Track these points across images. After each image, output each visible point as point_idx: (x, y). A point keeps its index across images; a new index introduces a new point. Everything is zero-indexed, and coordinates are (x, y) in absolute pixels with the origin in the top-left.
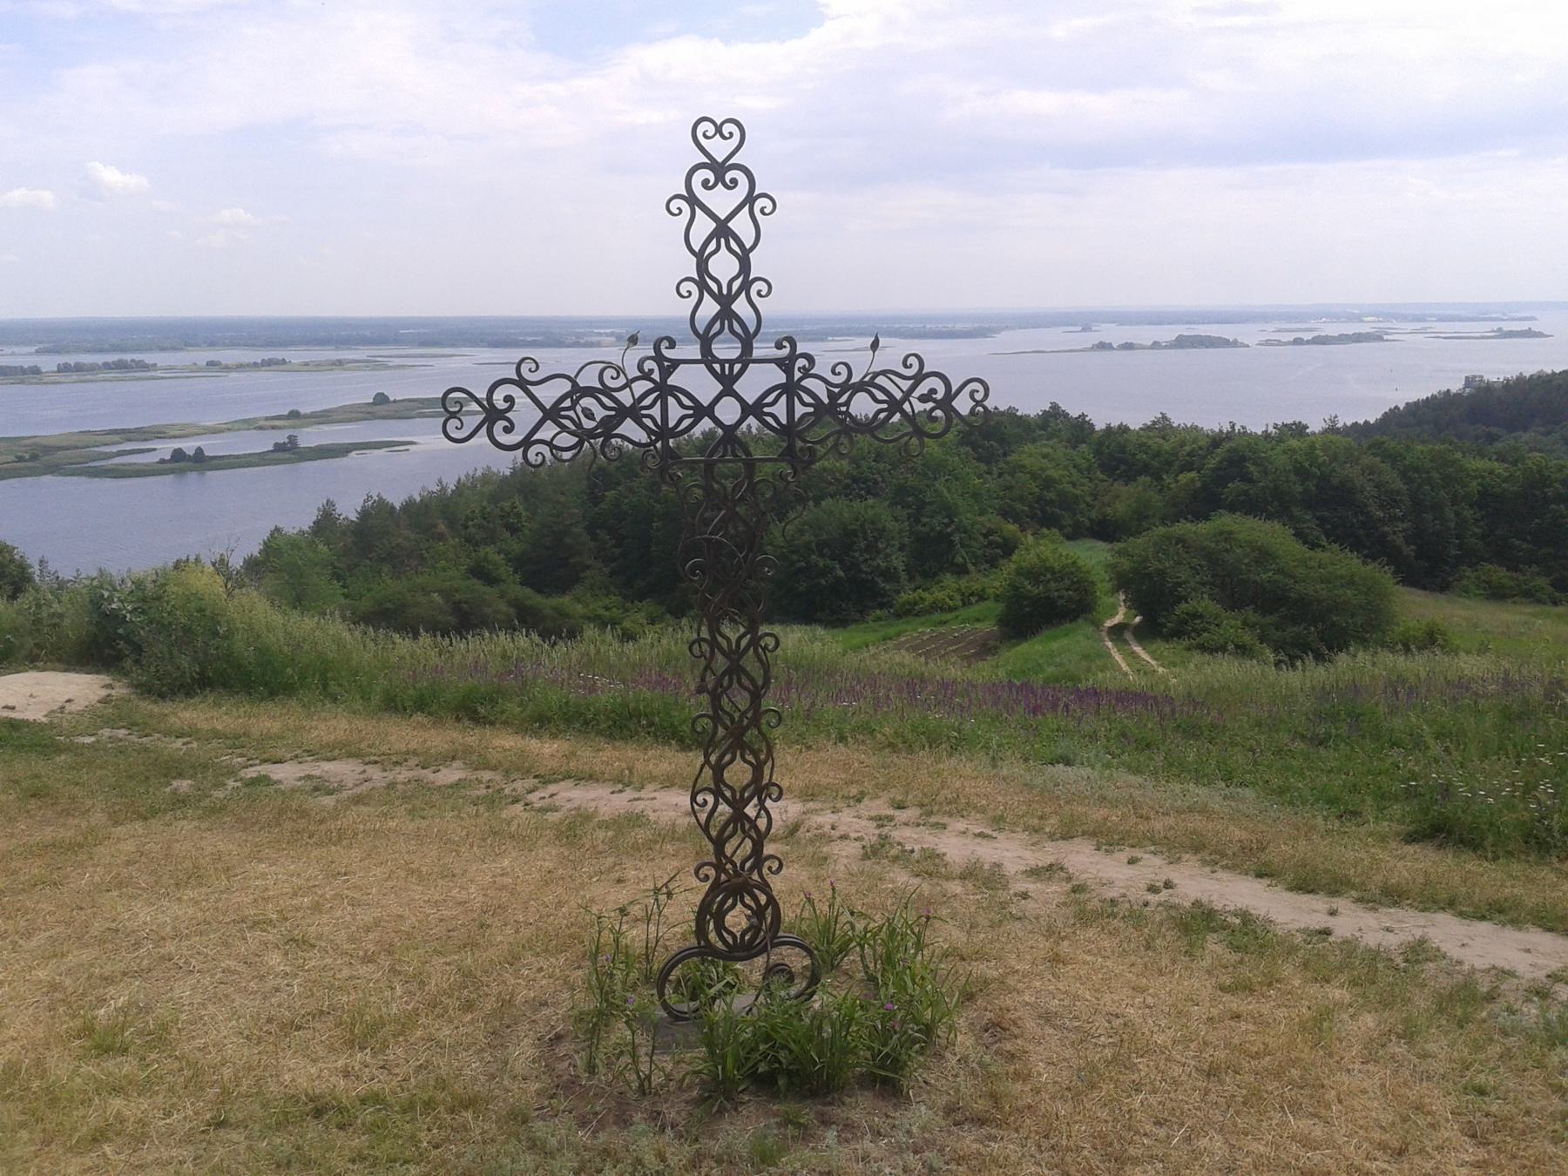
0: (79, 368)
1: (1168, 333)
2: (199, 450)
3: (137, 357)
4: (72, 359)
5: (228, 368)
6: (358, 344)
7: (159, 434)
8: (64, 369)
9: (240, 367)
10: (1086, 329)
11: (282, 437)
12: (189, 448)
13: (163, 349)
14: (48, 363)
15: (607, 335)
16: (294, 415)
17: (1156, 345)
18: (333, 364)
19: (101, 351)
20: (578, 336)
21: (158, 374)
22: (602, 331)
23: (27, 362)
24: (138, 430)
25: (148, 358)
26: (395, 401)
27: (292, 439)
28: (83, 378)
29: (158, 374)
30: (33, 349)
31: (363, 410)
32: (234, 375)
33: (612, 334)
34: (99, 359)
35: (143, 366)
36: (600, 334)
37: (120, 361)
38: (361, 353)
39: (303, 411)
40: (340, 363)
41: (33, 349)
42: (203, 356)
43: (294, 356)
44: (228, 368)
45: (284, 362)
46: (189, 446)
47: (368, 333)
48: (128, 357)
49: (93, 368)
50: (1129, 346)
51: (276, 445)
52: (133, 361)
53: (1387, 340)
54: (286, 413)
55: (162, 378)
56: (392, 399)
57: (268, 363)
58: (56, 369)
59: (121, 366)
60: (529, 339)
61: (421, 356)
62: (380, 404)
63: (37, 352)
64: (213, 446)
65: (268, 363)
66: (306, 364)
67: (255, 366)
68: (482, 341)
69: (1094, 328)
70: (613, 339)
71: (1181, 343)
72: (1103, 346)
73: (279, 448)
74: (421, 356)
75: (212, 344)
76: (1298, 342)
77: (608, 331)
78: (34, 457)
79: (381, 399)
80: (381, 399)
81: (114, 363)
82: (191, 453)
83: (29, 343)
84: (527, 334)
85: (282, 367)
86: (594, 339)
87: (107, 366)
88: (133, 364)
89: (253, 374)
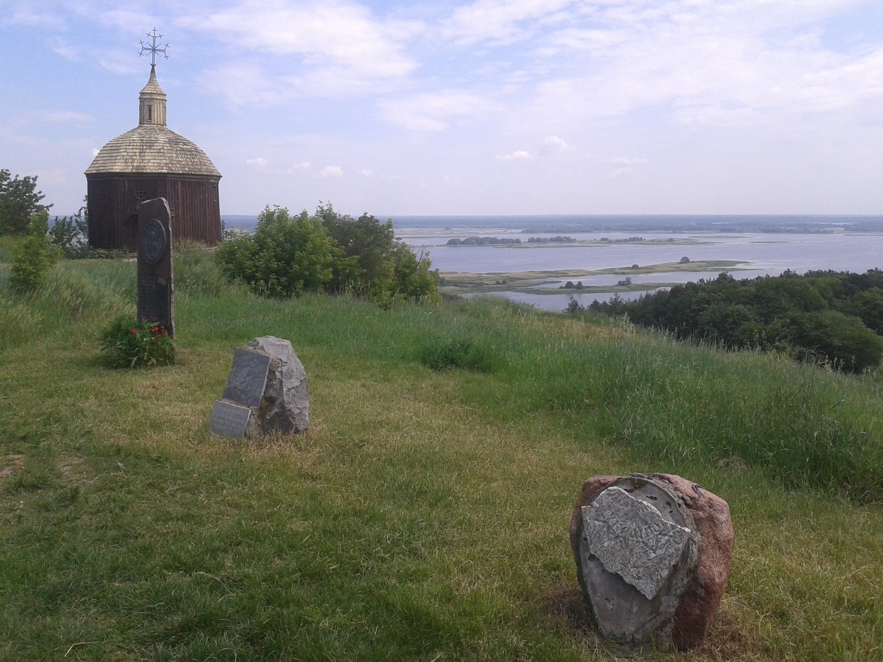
0: (538, 240)
2: (580, 283)
3: (567, 235)
4: (535, 236)
5: (611, 242)
6: (686, 230)
7: (565, 274)
8: (531, 241)
9: (618, 242)
11: (623, 278)
12: (575, 282)
13: (582, 232)
14: (524, 238)
16: (635, 267)
18: (668, 241)
19: (552, 232)
21: (576, 244)
23: (514, 237)
24: (556, 272)
25: (572, 236)
26: (693, 262)
27: (628, 280)
28: (540, 245)
29: (576, 244)
30: (520, 231)
31: (674, 266)
32: (614, 246)
34: (549, 236)
35: (569, 240)
37: (558, 237)
39: (640, 266)
40: (671, 241)
41: (520, 231)
42: (599, 236)
43: (648, 236)
44: (611, 242)
46: (575, 281)
48: (562, 235)
49: (545, 241)
51: (620, 282)
54: (631, 266)
55: (577, 246)
57: (632, 240)
58: (528, 241)
59: (558, 240)
61: (719, 237)
62: (684, 263)
63: (522, 232)
65: (632, 240)
66: (653, 241)
67: (625, 241)
73: (621, 284)
74: (719, 237)
75: (608, 229)
78: (504, 283)
79: (685, 260)
80: (685, 260)
81: (555, 238)
82: (576, 284)
83: (518, 228)
85: (639, 242)
87: (552, 240)
88: (564, 239)
89: (623, 245)
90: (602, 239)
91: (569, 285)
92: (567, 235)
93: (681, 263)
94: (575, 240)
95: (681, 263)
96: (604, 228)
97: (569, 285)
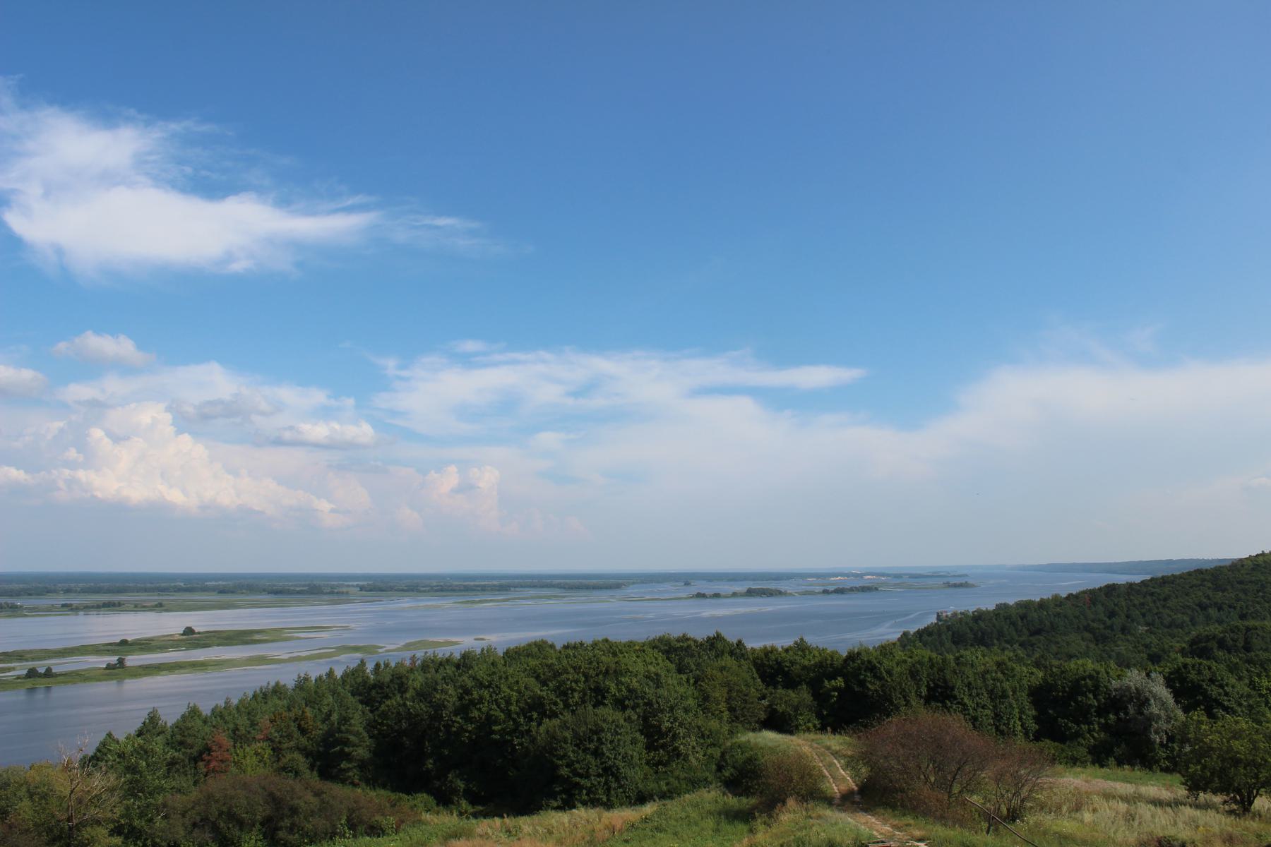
1: (741, 588)
2: (49, 670)
3: (9, 601)
7: (20, 656)
10: (687, 584)
11: (113, 659)
15: (353, 586)
16: (124, 642)
17: (735, 595)
18: (156, 606)
20: (332, 587)
22: (351, 583)
26: (199, 633)
27: (121, 661)
33: (357, 586)
36: (348, 586)
42: (60, 600)
45: (119, 604)
46: (41, 667)
47: (182, 584)
50: (717, 596)
51: (108, 665)
52: (6, 603)
53: (881, 590)
54: (118, 641)
56: (196, 631)
60: (298, 589)
64: (59, 666)
68: (264, 590)
69: (692, 584)
70: (359, 589)
72: (701, 596)
73: (109, 667)
75: (68, 591)
76: (825, 592)
77: (355, 583)
79: (189, 631)
80: (189, 631)
82: (42, 670)
84: (296, 586)
85: (118, 608)
86: (345, 590)
90: (63, 606)
91: (32, 673)
92: (9, 601)
93: (182, 635)
94: (21, 606)
95: (182, 635)
96: (62, 590)
97: (32, 673)
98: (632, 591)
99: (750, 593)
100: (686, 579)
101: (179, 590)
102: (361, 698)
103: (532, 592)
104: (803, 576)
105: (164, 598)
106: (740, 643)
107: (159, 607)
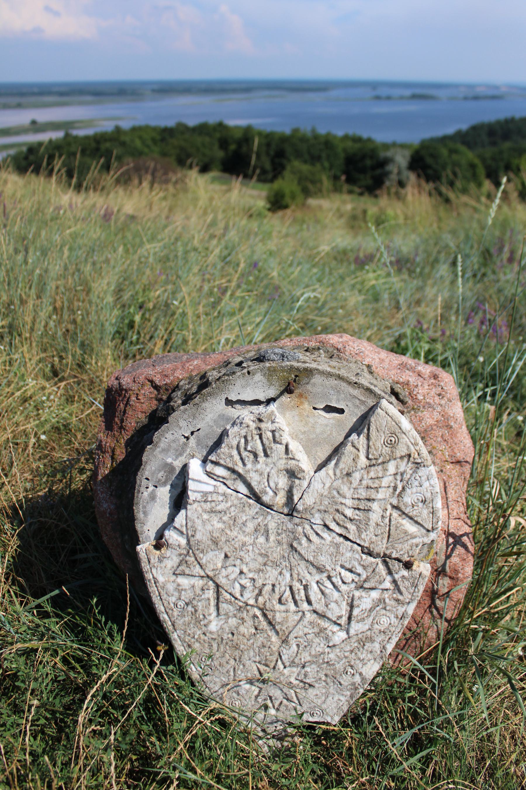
1: (408, 93)
17: (402, 98)
38: (33, 99)
50: (389, 98)
71: (415, 97)
79: (34, 122)
80: (34, 122)
98: (334, 93)
99: (415, 97)
100: (374, 85)
101: (34, 94)
102: (32, 168)
103: (266, 93)
104: (456, 86)
105: (24, 100)
106: (313, 131)
107: (19, 106)
